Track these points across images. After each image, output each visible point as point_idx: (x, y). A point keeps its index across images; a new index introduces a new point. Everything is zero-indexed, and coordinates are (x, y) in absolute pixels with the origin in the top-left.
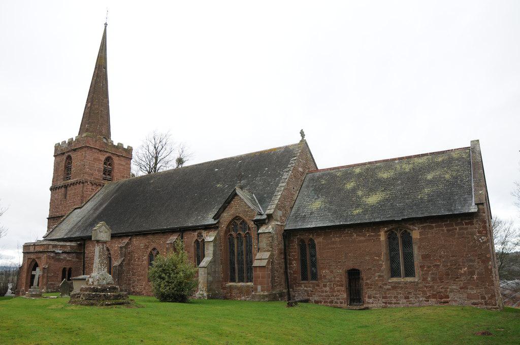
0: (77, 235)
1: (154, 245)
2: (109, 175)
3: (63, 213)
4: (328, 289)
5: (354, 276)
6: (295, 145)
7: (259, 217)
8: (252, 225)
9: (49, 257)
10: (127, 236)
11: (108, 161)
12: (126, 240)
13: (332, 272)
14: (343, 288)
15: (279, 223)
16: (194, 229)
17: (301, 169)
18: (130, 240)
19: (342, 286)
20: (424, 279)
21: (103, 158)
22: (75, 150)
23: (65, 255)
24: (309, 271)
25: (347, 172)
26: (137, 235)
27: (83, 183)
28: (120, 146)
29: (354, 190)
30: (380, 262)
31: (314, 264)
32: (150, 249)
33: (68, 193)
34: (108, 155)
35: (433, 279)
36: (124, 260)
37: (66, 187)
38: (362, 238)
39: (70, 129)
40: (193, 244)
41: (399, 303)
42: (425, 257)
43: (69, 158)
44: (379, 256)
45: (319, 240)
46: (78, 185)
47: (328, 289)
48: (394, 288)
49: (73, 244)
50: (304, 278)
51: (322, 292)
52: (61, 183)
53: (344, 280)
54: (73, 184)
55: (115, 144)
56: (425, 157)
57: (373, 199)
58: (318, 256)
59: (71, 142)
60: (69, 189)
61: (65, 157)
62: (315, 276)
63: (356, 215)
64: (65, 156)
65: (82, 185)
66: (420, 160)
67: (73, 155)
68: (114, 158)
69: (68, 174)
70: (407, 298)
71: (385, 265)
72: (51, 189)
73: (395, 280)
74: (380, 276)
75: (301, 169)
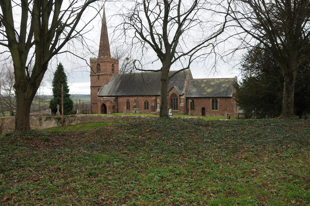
1: (146, 99)
4: (197, 112)
5: (203, 109)
7: (180, 94)
8: (178, 96)
9: (110, 102)
12: (136, 98)
24: (193, 108)
29: (204, 87)
33: (100, 78)
35: (222, 111)
37: (98, 76)
42: (220, 106)
43: (99, 64)
45: (195, 100)
46: (105, 75)
47: (197, 112)
53: (201, 110)
62: (194, 109)
67: (101, 64)
68: (115, 64)
72: (90, 76)
73: (213, 110)
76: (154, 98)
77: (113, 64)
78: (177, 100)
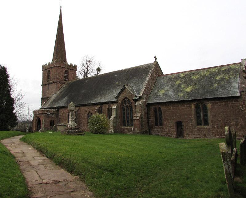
0: (56, 106)
1: (90, 110)
2: (67, 78)
3: (48, 96)
4: (167, 130)
5: (179, 124)
6: (152, 63)
8: (132, 101)
10: (78, 106)
11: (66, 72)
13: (169, 122)
14: (174, 130)
15: (144, 100)
16: (107, 103)
17: (155, 75)
18: (79, 108)
19: (174, 129)
20: (213, 127)
21: (64, 71)
22: (51, 68)
23: (51, 115)
24: (159, 122)
25: (177, 76)
26: (82, 106)
27: (56, 83)
28: (71, 65)
29: (180, 84)
30: (192, 119)
31: (161, 119)
32: (88, 112)
33: (50, 87)
34: (66, 69)
35: (218, 127)
36: (76, 117)
38: (183, 107)
39: (48, 58)
40: (107, 110)
41: (201, 138)
43: (49, 71)
44: (191, 115)
45: (163, 108)
47: (167, 130)
48: (198, 130)
49: (54, 110)
50: (157, 125)
51: (165, 131)
52: (45, 83)
54: (52, 83)
55: (69, 64)
56: (216, 68)
57: (189, 89)
58: (163, 115)
59: (49, 64)
60: (50, 85)
61: (47, 71)
62: (161, 124)
63: (180, 97)
64: (47, 70)
65: (55, 83)
66: (214, 70)
67: (51, 70)
68: (69, 71)
69: (49, 78)
70: (204, 135)
71: (194, 120)
72: (42, 85)
73: (199, 127)
74: (191, 125)
75: (155, 75)
76: (98, 107)
77: (66, 71)
78: (131, 110)
